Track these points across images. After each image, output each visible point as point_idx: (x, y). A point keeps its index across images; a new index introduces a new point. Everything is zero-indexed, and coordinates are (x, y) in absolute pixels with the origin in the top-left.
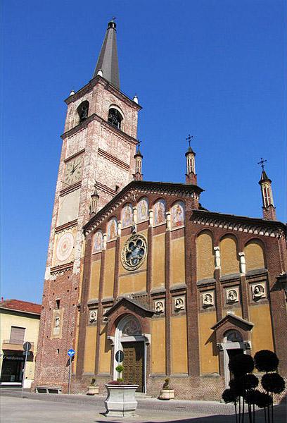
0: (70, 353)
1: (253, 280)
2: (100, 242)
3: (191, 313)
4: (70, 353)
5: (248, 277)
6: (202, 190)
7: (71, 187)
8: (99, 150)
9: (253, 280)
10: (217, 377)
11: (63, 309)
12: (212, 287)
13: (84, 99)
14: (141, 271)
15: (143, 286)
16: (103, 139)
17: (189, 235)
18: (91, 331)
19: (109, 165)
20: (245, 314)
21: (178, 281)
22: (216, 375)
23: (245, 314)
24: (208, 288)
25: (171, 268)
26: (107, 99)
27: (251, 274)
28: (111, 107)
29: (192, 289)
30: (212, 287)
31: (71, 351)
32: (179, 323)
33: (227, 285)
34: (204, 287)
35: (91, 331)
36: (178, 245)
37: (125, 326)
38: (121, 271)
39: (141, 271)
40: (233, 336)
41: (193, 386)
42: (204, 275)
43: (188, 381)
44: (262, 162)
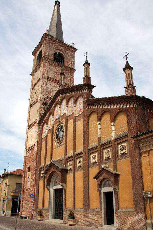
0: (31, 196)
1: (119, 142)
2: (46, 129)
3: (88, 165)
4: (31, 196)
5: (116, 140)
6: (94, 87)
7: (34, 101)
8: (48, 77)
9: (119, 142)
10: (98, 211)
11: (31, 172)
12: (96, 150)
13: (40, 50)
14: (62, 145)
15: (63, 154)
16: (51, 71)
17: (87, 117)
18: (41, 182)
19: (55, 86)
20: (115, 168)
21: (80, 149)
22: (98, 210)
23: (115, 168)
24: (94, 151)
25: (77, 140)
26: (52, 46)
27: (118, 137)
28: (56, 51)
29: (89, 151)
30: (96, 150)
31: (32, 195)
32: (80, 174)
33: (105, 147)
34: (92, 150)
35: (41, 182)
36: (80, 124)
37: (56, 180)
38: (55, 146)
39: (62, 145)
40: (107, 183)
41: (85, 217)
42: (93, 143)
43: (83, 213)
44: (126, 55)
